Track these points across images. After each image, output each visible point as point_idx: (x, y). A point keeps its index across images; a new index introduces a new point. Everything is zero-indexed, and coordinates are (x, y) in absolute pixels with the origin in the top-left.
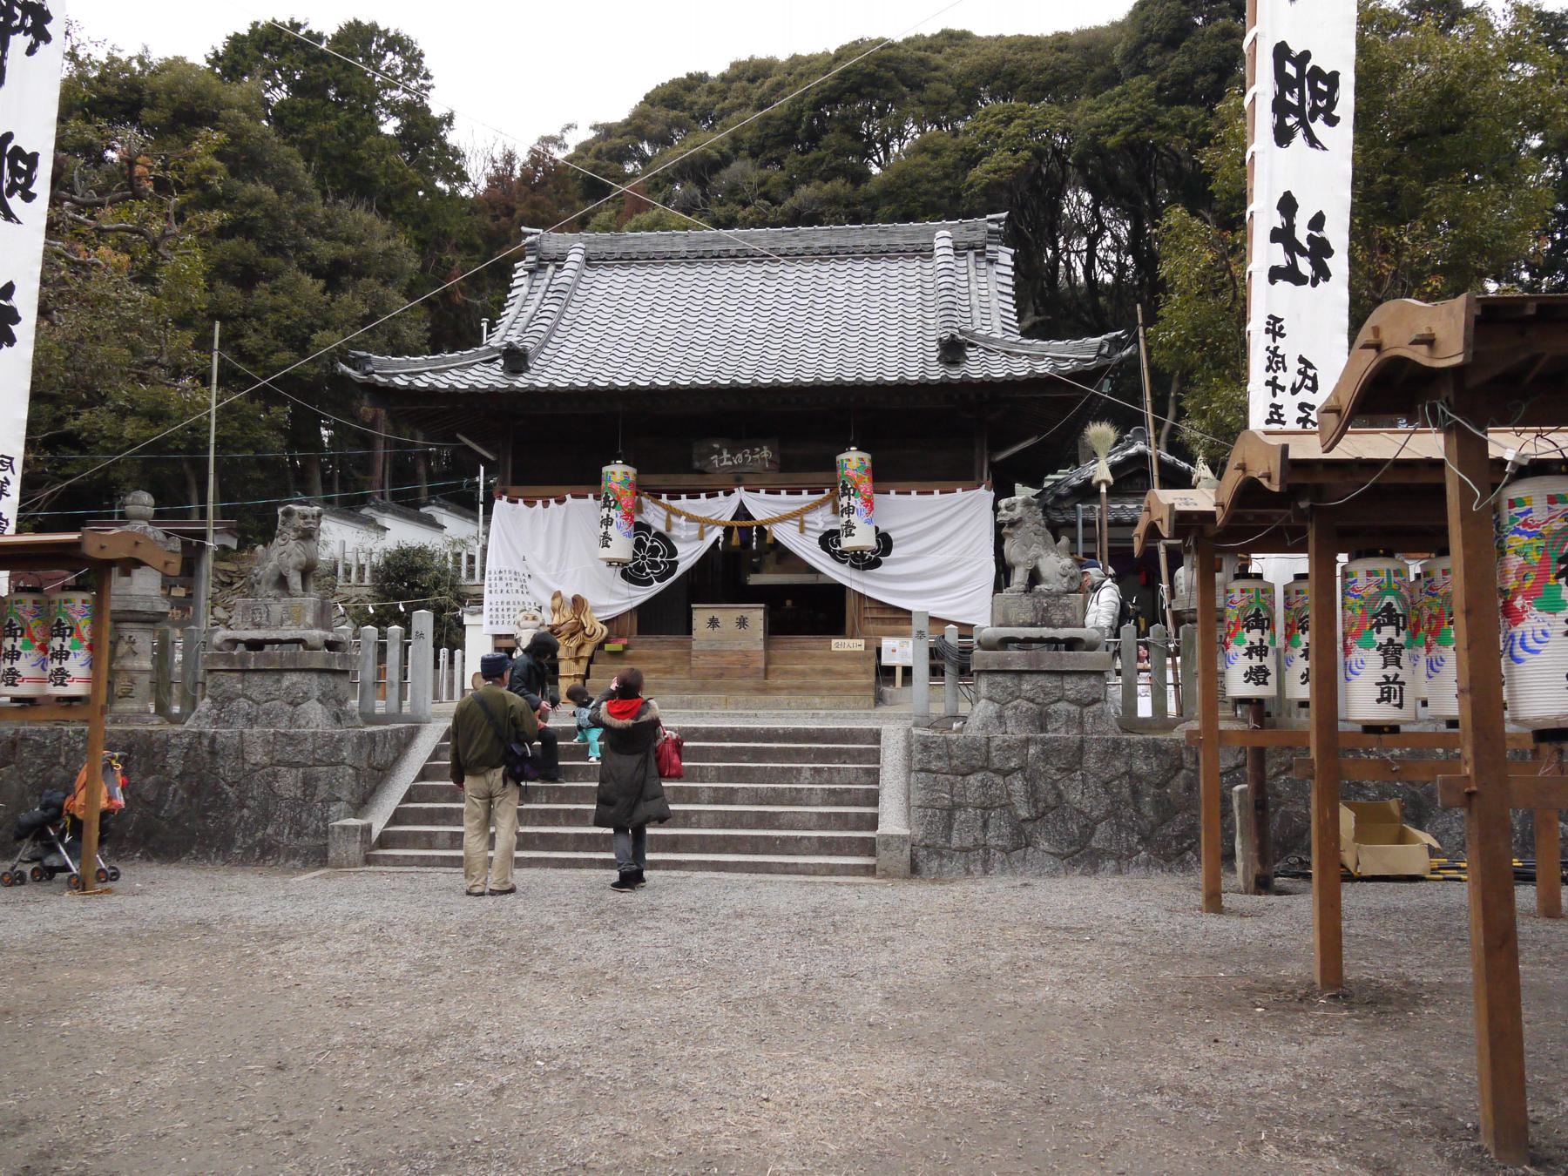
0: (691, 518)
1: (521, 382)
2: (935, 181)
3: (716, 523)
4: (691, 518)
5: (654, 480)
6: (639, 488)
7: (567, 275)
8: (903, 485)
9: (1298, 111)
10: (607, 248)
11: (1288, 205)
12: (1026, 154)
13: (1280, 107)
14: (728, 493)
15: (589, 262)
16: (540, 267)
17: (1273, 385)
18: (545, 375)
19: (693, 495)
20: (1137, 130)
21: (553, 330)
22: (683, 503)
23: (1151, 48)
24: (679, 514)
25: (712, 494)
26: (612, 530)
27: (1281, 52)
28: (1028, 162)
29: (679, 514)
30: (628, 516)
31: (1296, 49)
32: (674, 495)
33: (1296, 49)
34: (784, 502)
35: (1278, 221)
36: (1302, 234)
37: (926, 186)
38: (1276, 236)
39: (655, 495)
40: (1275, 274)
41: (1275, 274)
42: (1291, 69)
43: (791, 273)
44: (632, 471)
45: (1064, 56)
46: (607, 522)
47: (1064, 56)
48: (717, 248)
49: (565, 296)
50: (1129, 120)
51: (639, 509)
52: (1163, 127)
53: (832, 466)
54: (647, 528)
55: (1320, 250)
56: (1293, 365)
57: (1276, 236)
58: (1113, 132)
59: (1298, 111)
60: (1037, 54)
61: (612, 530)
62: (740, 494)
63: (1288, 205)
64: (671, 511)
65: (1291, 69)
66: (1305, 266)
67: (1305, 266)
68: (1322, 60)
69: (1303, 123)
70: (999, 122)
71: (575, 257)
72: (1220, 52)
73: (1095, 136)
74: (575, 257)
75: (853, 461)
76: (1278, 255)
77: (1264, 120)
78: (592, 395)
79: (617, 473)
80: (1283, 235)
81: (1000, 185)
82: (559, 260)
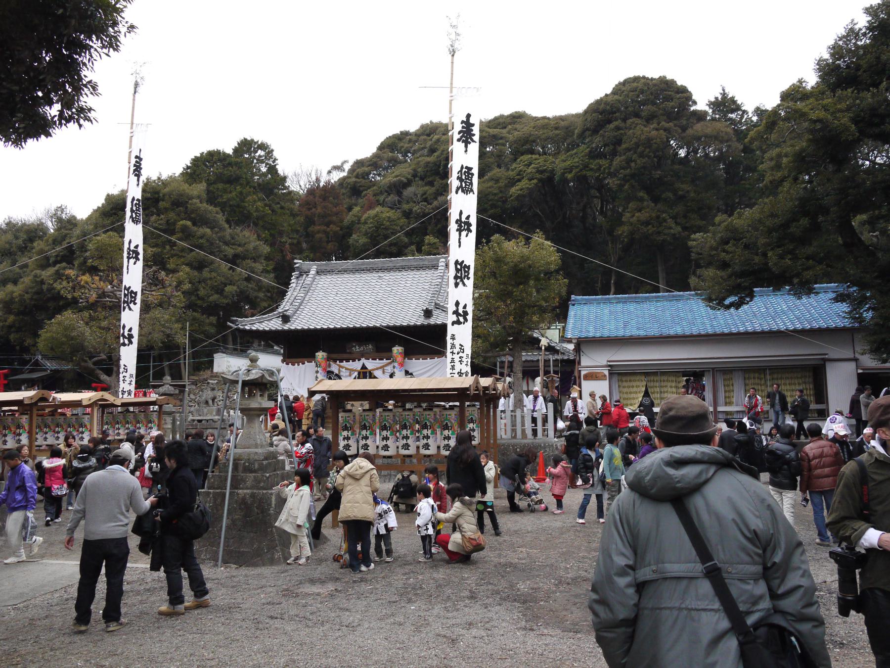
0: (347, 369)
1: (286, 327)
2: (495, 194)
3: (355, 371)
4: (347, 369)
5: (334, 356)
6: (328, 359)
7: (309, 280)
8: (418, 356)
9: (461, 278)
10: (324, 267)
11: (457, 304)
12: (535, 181)
13: (456, 277)
14: (359, 360)
15: (318, 273)
16: (301, 275)
17: (453, 353)
18: (296, 324)
19: (348, 361)
20: (581, 170)
21: (301, 304)
22: (344, 364)
23: (588, 133)
24: (343, 367)
25: (354, 360)
26: (319, 375)
27: (457, 262)
28: (536, 184)
29: (343, 367)
30: (324, 369)
31: (460, 261)
32: (341, 361)
33: (460, 261)
34: (378, 363)
35: (455, 308)
36: (461, 311)
37: (491, 197)
38: (454, 313)
39: (335, 361)
40: (453, 323)
41: (453, 323)
42: (459, 267)
43: (387, 276)
44: (325, 354)
45: (557, 132)
46: (317, 372)
47: (557, 132)
48: (363, 267)
49: (307, 290)
50: (577, 167)
51: (330, 366)
52: (591, 169)
53: (391, 351)
54: (332, 372)
55: (466, 313)
56: (458, 347)
57: (454, 313)
58: (570, 172)
59: (461, 278)
60: (545, 131)
61: (319, 375)
62: (363, 360)
63: (457, 304)
64: (340, 366)
65: (459, 267)
66: (461, 319)
67: (461, 319)
68: (467, 263)
69: (462, 281)
70: (525, 165)
71: (313, 272)
72: (615, 137)
73: (563, 174)
74: (313, 272)
75: (397, 350)
76: (454, 318)
77: (452, 281)
78: (309, 331)
79: (320, 355)
80: (456, 312)
81: (524, 196)
82: (307, 272)
